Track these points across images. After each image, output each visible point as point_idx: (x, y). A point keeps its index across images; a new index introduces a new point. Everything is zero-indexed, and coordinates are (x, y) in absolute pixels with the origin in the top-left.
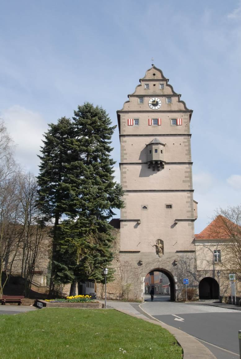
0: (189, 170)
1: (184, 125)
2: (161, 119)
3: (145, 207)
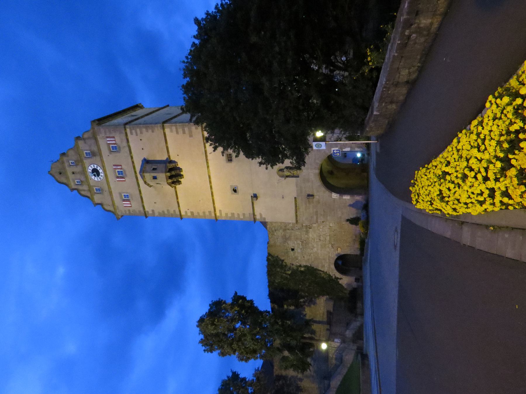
2: (114, 165)
3: (235, 191)
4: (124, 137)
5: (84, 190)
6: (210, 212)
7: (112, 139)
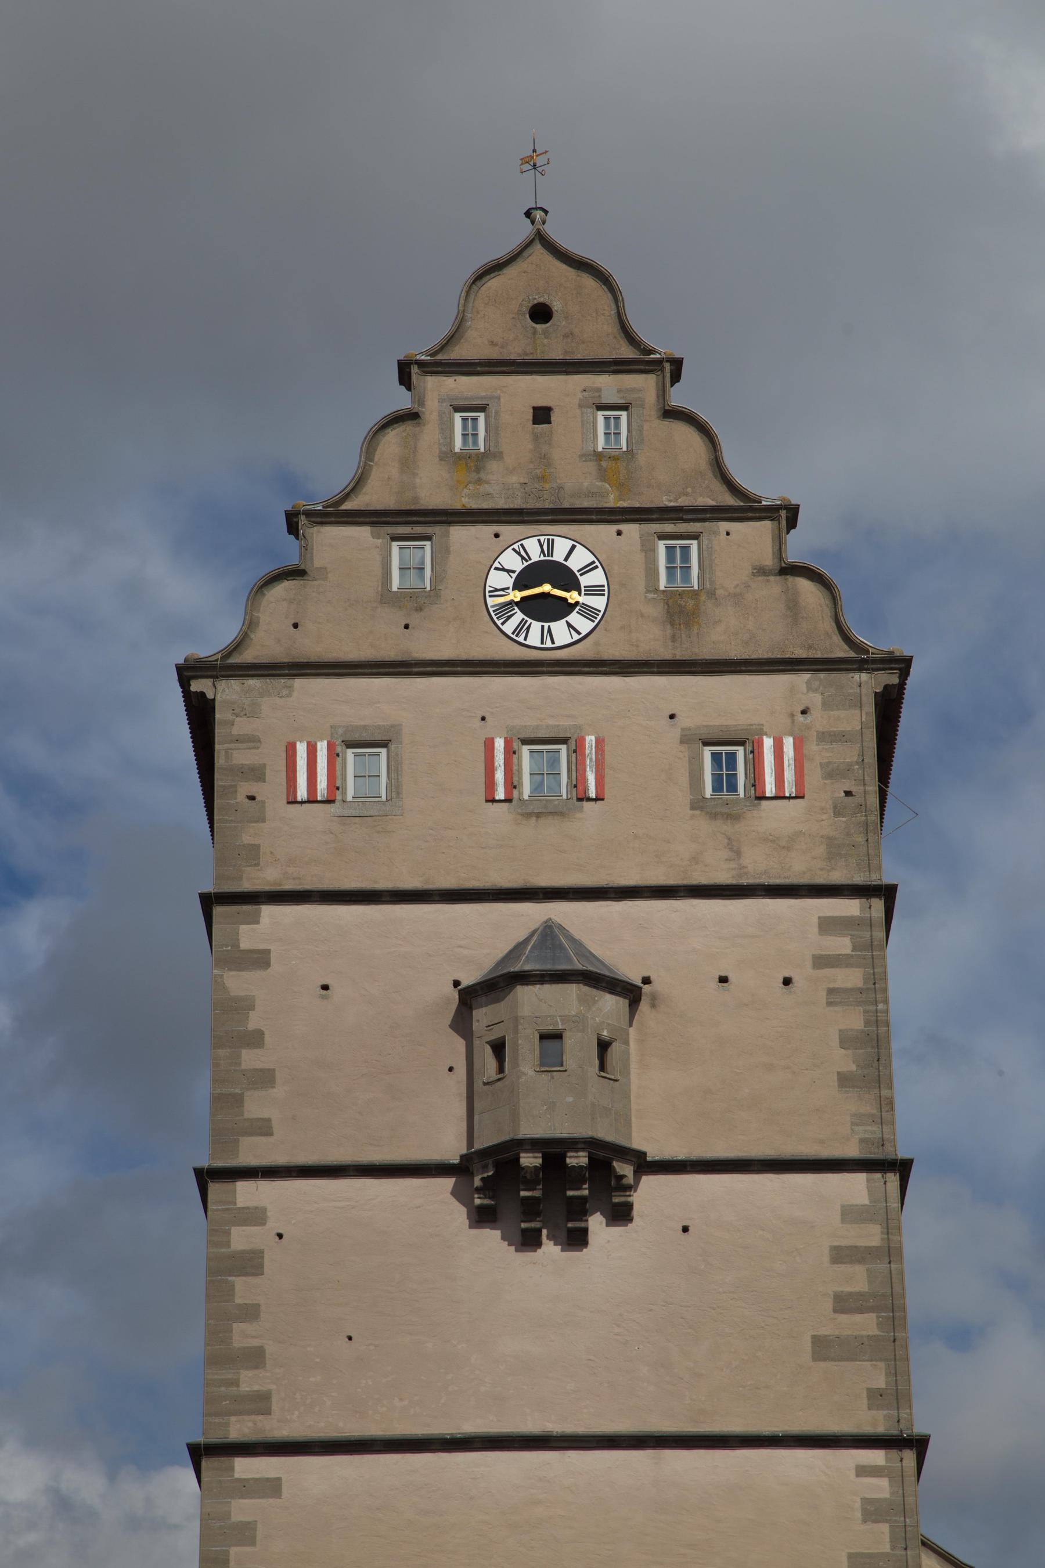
0: (872, 1236)
1: (823, 792)
4: (800, 868)
5: (408, 463)
6: (261, 1403)
7: (789, 775)
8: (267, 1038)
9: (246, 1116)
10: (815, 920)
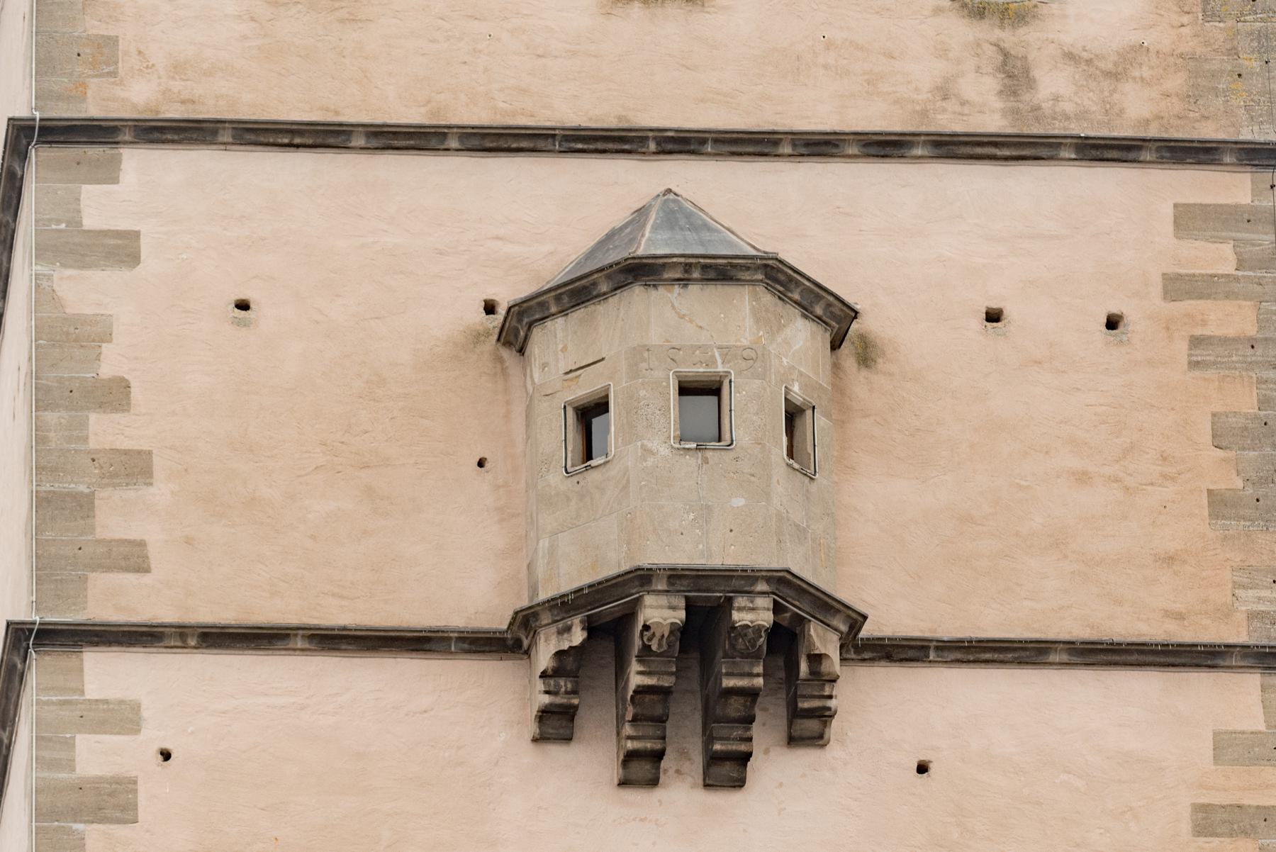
8: (136, 392)
9: (100, 534)
10: (1168, 211)
